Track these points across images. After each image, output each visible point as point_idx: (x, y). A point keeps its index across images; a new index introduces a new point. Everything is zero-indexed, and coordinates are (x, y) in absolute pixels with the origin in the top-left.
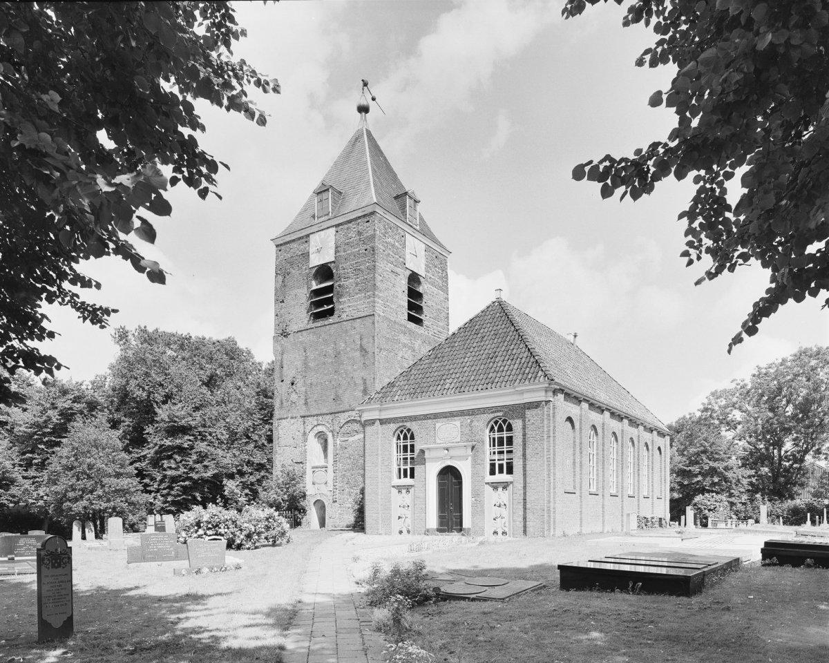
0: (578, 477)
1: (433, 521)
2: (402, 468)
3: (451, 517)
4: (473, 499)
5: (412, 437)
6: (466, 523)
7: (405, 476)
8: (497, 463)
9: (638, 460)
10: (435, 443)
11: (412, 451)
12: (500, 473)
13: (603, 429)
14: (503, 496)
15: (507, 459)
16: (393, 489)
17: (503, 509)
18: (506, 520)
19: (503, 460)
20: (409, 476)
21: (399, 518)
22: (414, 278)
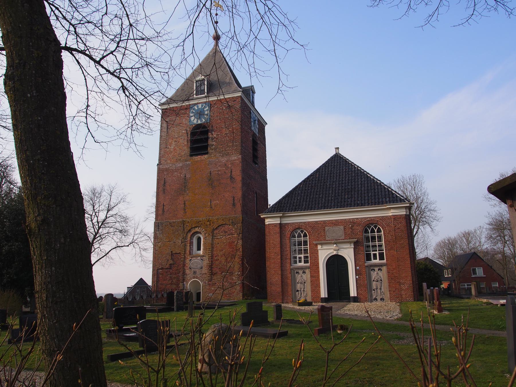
4: (357, 277)
6: (353, 292)
7: (300, 262)
8: (372, 253)
10: (325, 240)
12: (374, 259)
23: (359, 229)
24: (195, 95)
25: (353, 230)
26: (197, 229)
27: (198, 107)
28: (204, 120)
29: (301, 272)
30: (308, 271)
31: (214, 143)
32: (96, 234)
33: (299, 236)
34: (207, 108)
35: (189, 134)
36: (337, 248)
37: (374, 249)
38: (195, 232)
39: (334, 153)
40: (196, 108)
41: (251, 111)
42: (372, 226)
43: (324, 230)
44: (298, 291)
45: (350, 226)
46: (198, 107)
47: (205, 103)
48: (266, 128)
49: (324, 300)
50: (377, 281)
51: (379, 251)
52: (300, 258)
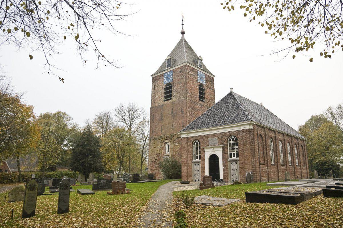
0: (265, 158)
2: (196, 155)
4: (224, 167)
5: (200, 144)
6: (221, 177)
7: (197, 158)
8: (232, 153)
9: (299, 152)
11: (200, 149)
12: (233, 157)
13: (275, 139)
14: (234, 166)
15: (236, 152)
16: (193, 164)
18: (237, 175)
19: (235, 152)
20: (198, 158)
21: (195, 175)
22: (201, 85)
23: (225, 138)
25: (222, 139)
26: (167, 141)
27: (167, 74)
29: (197, 164)
30: (200, 164)
31: (174, 93)
32: (145, 143)
34: (172, 74)
35: (164, 89)
36: (213, 151)
37: (234, 150)
38: (166, 142)
39: (230, 92)
40: (166, 74)
41: (198, 71)
42: (233, 137)
43: (208, 140)
44: (195, 175)
45: (221, 137)
46: (167, 74)
47: (170, 71)
50: (234, 170)
51: (236, 152)
52: (197, 156)
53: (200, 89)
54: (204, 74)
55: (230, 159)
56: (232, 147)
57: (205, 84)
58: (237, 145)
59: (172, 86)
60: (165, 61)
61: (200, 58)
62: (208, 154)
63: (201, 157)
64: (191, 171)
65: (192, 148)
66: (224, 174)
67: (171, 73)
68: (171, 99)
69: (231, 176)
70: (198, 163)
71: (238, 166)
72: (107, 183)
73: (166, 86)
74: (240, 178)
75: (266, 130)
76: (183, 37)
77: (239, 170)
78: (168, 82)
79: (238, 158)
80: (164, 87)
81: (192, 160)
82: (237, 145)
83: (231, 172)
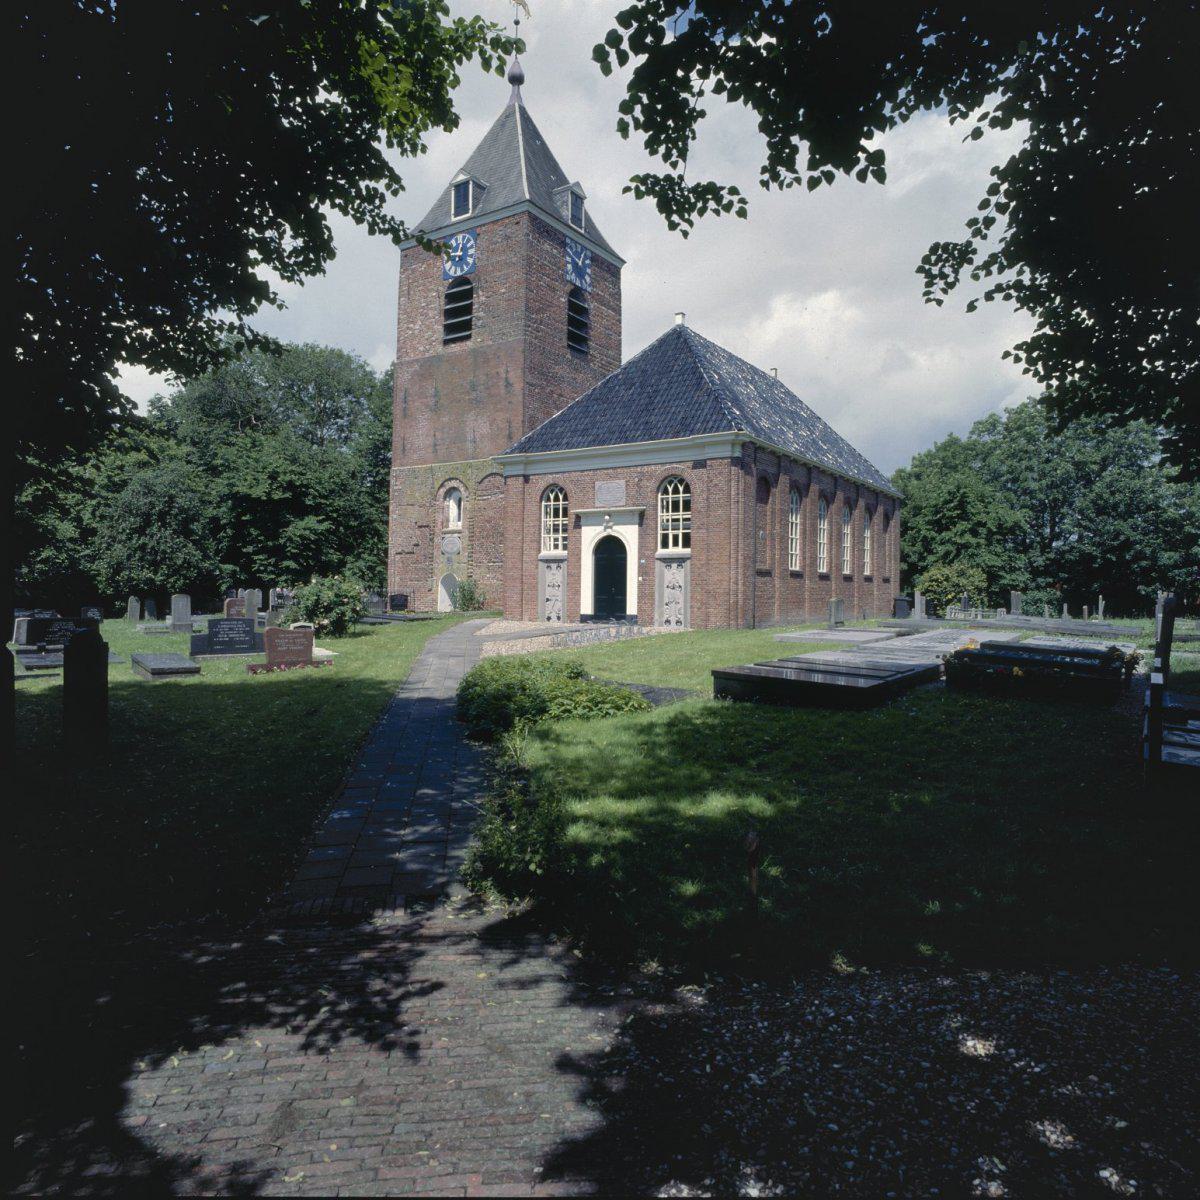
1: (587, 606)
3: (610, 600)
4: (640, 578)
6: (632, 608)
11: (565, 514)
14: (676, 575)
16: (541, 564)
17: (678, 590)
18: (681, 605)
21: (548, 600)
24: (453, 216)
26: (454, 484)
28: (466, 269)
29: (554, 566)
33: (676, 491)
34: (472, 242)
35: (443, 298)
43: (594, 487)
44: (548, 600)
45: (637, 480)
48: (622, 270)
49: (585, 619)
51: (684, 529)
53: (572, 306)
54: (589, 253)
55: (661, 552)
56: (671, 515)
57: (589, 289)
58: (687, 506)
59: (471, 290)
60: (447, 193)
61: (576, 190)
62: (591, 535)
63: (572, 546)
64: (535, 587)
65: (540, 510)
66: (641, 597)
67: (469, 241)
68: (468, 337)
69: (661, 606)
70: (558, 561)
71: (686, 574)
72: (244, 632)
73: (452, 286)
74: (692, 612)
75: (782, 464)
76: (517, 96)
77: (689, 588)
78: (459, 273)
79: (688, 551)
80: (443, 290)
81: (539, 551)
82: (687, 506)
83: (661, 596)
